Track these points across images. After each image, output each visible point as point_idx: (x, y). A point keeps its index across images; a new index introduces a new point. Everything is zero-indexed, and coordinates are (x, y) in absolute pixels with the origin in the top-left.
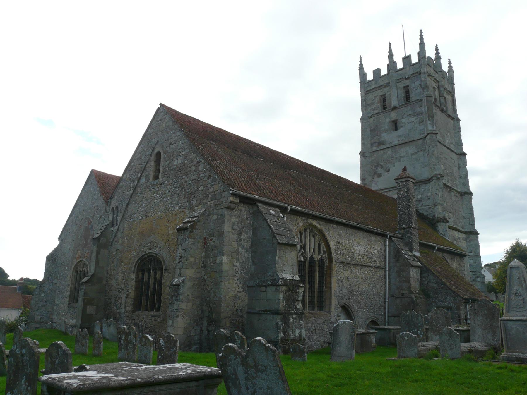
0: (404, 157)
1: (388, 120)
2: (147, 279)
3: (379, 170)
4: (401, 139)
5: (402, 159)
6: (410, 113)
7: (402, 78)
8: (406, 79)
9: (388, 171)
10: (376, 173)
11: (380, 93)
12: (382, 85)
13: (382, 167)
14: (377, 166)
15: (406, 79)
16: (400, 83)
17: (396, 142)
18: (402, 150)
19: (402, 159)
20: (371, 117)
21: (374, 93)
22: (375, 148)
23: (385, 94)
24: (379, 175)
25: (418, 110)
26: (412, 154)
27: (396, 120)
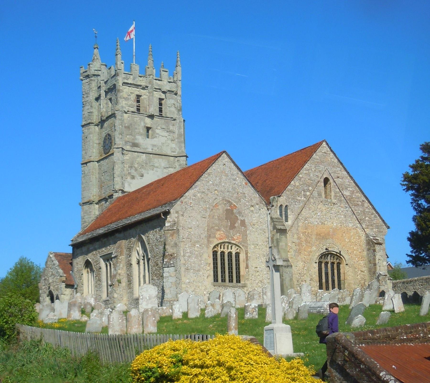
0: (157, 167)
1: (143, 124)
2: (343, 277)
3: (133, 172)
4: (155, 148)
5: (155, 169)
6: (164, 127)
7: (160, 89)
8: (164, 92)
9: (142, 176)
10: (129, 173)
11: (137, 91)
12: (140, 86)
13: (136, 170)
14: (131, 167)
15: (164, 92)
16: (156, 92)
17: (150, 150)
18: (156, 160)
19: (155, 169)
20: (126, 113)
21: (130, 88)
22: (128, 148)
23: (141, 96)
24: (133, 177)
25: (171, 128)
26: (165, 168)
27: (150, 128)
